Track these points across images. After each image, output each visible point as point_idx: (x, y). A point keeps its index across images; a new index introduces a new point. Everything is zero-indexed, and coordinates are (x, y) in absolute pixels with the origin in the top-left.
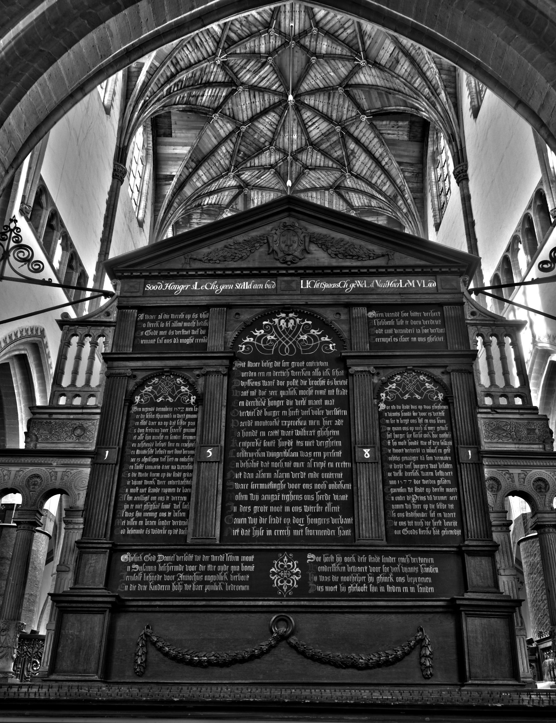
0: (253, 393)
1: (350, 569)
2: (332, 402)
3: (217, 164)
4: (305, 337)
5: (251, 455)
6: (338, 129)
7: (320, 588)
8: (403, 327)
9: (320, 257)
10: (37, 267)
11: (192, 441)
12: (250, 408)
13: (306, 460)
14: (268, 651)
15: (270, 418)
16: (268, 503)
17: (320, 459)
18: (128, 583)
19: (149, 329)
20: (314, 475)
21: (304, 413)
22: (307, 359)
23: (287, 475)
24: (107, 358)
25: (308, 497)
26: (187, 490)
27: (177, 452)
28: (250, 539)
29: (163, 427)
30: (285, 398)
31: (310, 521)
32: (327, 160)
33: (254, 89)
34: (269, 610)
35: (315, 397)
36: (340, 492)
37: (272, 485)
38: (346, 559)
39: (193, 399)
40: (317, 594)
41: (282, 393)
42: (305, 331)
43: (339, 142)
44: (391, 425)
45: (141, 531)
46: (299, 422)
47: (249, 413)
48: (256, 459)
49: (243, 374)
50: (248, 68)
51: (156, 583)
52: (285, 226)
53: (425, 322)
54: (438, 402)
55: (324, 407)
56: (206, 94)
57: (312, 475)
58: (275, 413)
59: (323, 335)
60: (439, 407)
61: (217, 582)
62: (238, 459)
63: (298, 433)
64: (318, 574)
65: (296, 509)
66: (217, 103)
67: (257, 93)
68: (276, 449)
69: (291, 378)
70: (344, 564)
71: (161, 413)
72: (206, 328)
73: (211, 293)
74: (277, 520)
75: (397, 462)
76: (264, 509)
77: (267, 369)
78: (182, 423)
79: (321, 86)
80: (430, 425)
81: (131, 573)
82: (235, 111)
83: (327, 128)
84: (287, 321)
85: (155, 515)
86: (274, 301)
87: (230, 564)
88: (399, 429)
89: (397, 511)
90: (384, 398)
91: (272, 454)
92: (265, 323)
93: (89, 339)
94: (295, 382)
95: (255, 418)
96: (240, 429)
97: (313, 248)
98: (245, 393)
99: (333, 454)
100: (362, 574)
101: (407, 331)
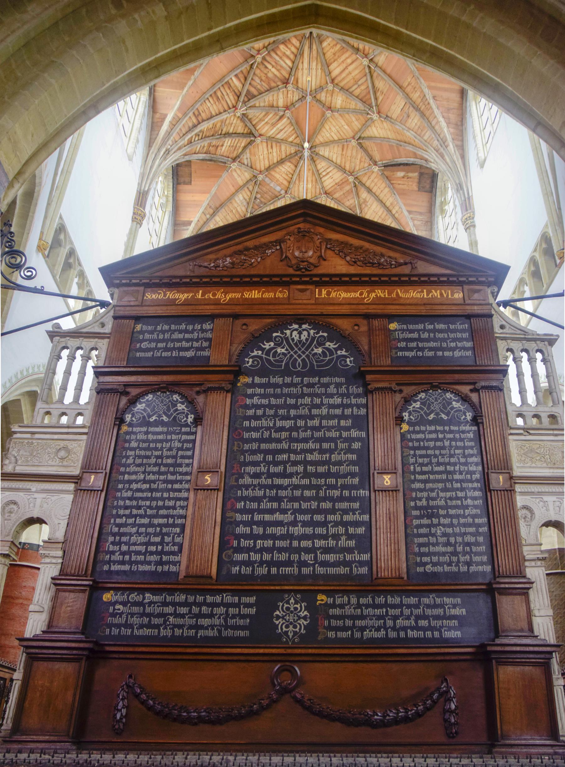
0: (260, 412)
2: (349, 422)
3: (234, 211)
4: (320, 350)
5: (256, 482)
6: (351, 179)
10: (29, 274)
12: (256, 429)
13: (318, 488)
15: (279, 441)
16: (274, 537)
17: (334, 487)
18: (110, 626)
19: (146, 340)
20: (327, 505)
21: (317, 434)
22: (321, 374)
23: (296, 505)
25: (319, 530)
26: (180, 521)
28: (252, 577)
30: (296, 418)
31: (322, 557)
33: (271, 140)
34: (271, 659)
35: (329, 417)
36: (356, 524)
37: (278, 517)
38: (363, 601)
40: (327, 640)
41: (293, 412)
42: (320, 344)
43: (352, 191)
44: (414, 448)
45: (126, 568)
46: (311, 445)
47: (254, 435)
48: (261, 486)
49: (250, 391)
50: (266, 120)
51: (141, 626)
55: (339, 428)
56: (225, 144)
58: (284, 435)
59: (340, 348)
60: (468, 428)
61: (212, 627)
63: (310, 457)
64: (329, 617)
65: (304, 544)
66: (236, 152)
67: (274, 144)
68: (284, 475)
69: (303, 396)
70: (359, 606)
71: (154, 433)
73: (217, 303)
74: (284, 557)
75: (421, 490)
76: (269, 543)
77: (276, 386)
78: (178, 445)
79: (336, 138)
81: (114, 615)
82: (253, 161)
83: (341, 178)
84: (300, 333)
85: (143, 549)
87: (228, 605)
88: (423, 452)
89: (420, 545)
90: (406, 418)
91: (278, 481)
92: (275, 335)
93: (79, 352)
94: (307, 400)
95: (261, 440)
96: (243, 452)
98: (251, 412)
99: (349, 481)
101: (432, 344)
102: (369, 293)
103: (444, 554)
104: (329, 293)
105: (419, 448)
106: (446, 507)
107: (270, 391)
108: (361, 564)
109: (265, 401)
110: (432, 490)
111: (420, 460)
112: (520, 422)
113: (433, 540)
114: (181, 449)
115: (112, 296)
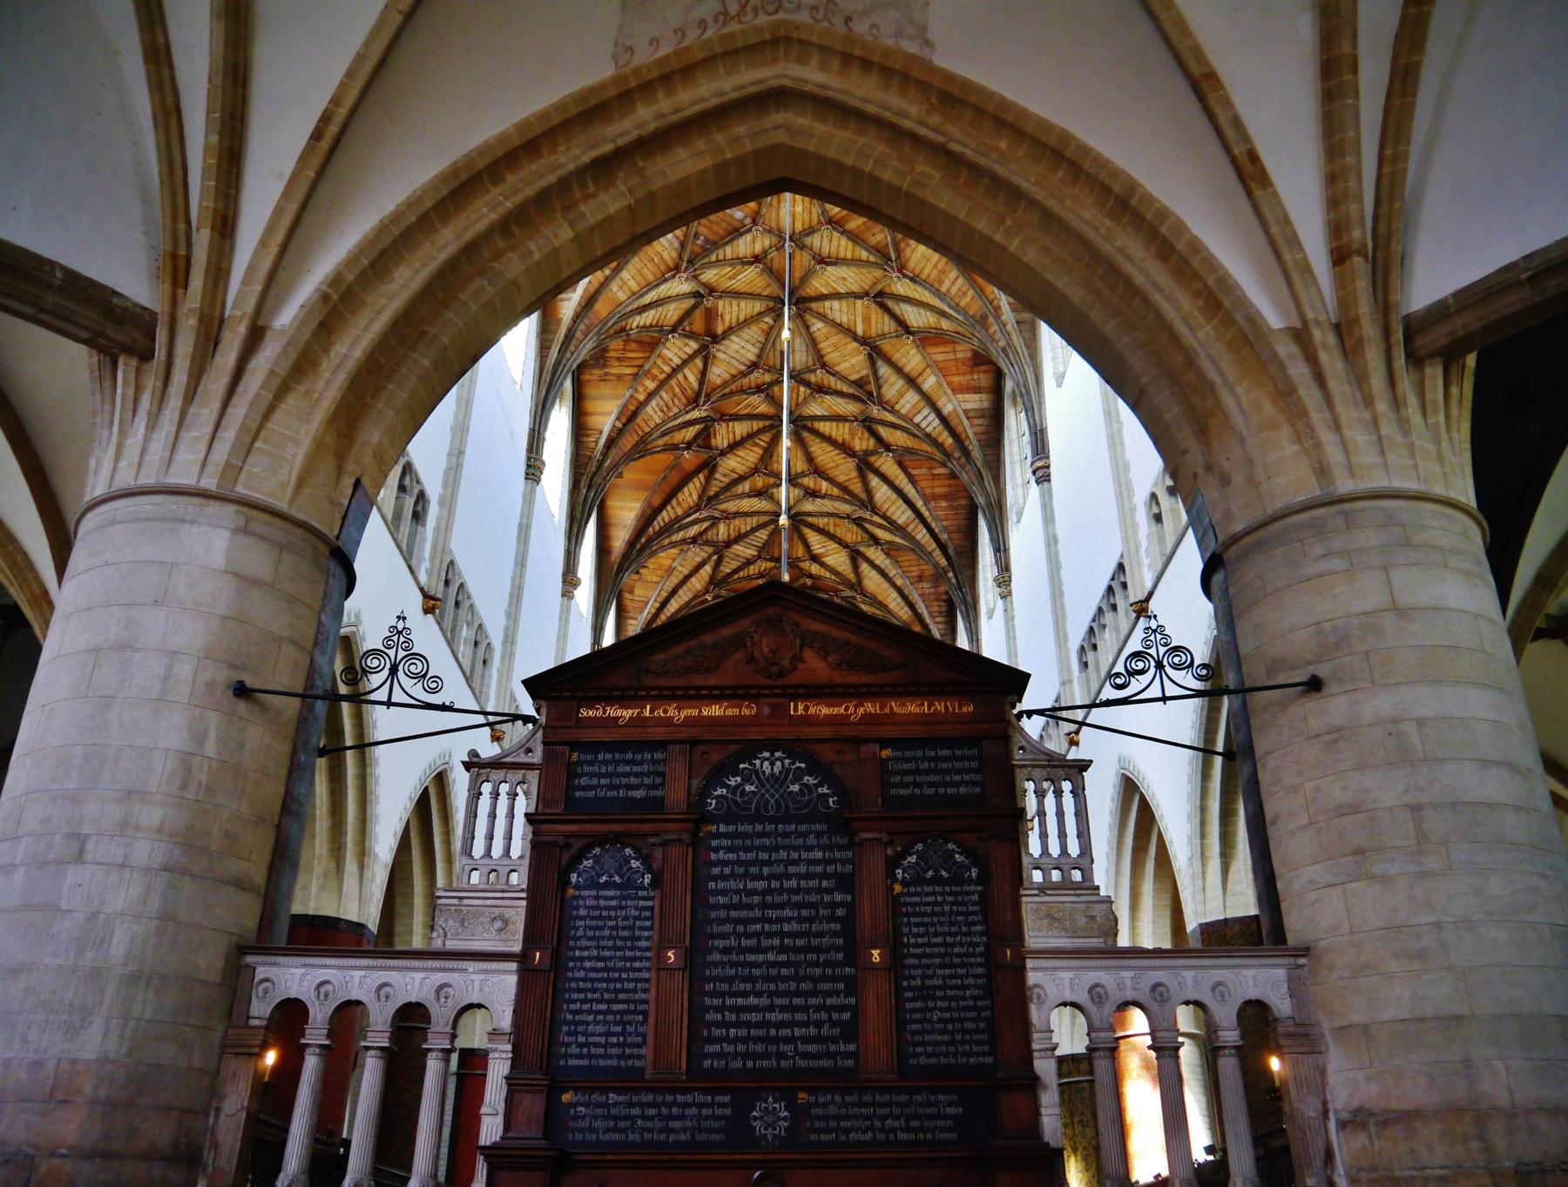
0: (727, 871)
5: (725, 958)
7: (814, 1137)
11: (647, 939)
12: (724, 893)
13: (796, 965)
15: (750, 907)
16: (748, 1025)
17: (815, 964)
18: (574, 1130)
21: (795, 899)
23: (772, 987)
25: (799, 1016)
26: (642, 1007)
27: (628, 954)
29: (609, 918)
30: (769, 877)
32: (857, 249)
35: (809, 876)
36: (841, 1009)
37: (752, 1000)
39: (647, 879)
41: (766, 870)
44: (908, 915)
45: (584, 1062)
46: (787, 912)
47: (721, 900)
48: (733, 964)
49: (714, 843)
51: (607, 1131)
54: (970, 881)
57: (803, 986)
58: (756, 899)
60: (972, 888)
61: (685, 1130)
63: (786, 928)
68: (758, 950)
69: (777, 848)
74: (760, 1048)
75: (915, 967)
76: (743, 1032)
77: (744, 836)
78: (634, 913)
80: (959, 913)
87: (700, 1106)
88: (918, 920)
91: (751, 958)
94: (783, 854)
98: (716, 871)
100: (866, 1118)
105: (915, 915)
106: (944, 988)
107: (738, 842)
108: (848, 1055)
109: (732, 856)
110: (928, 967)
111: (915, 930)
112: (1037, 876)
113: (927, 1026)
114: (637, 918)
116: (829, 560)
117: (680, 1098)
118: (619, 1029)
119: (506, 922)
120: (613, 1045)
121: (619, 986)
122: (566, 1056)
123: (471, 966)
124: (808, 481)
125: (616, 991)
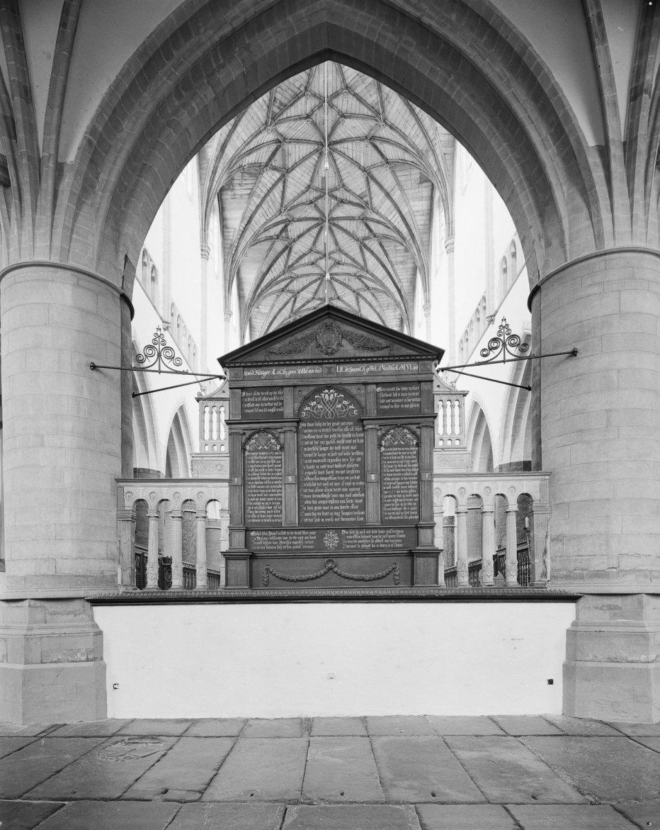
0: (311, 443)
1: (362, 537)
2: (355, 448)
4: (340, 406)
5: (312, 479)
8: (396, 398)
9: (348, 349)
11: (280, 472)
12: (310, 452)
13: (341, 481)
14: (324, 574)
15: (321, 458)
16: (322, 505)
17: (349, 481)
19: (249, 402)
20: (345, 490)
21: (340, 454)
22: (342, 420)
23: (331, 490)
24: (228, 423)
25: (342, 502)
26: (280, 499)
27: (272, 478)
28: (313, 524)
29: (264, 464)
30: (329, 445)
31: (343, 514)
35: (346, 445)
36: (359, 498)
37: (323, 496)
38: (361, 532)
39: (278, 447)
40: (347, 549)
41: (328, 443)
42: (340, 402)
44: (387, 460)
46: (337, 460)
47: (310, 455)
48: (315, 481)
49: (305, 431)
52: (326, 326)
53: (410, 394)
54: (413, 446)
55: (350, 451)
57: (344, 490)
58: (324, 455)
59: (350, 404)
60: (414, 449)
62: (305, 482)
63: (337, 466)
64: (347, 539)
65: (336, 508)
68: (325, 476)
69: (332, 433)
70: (360, 535)
71: (262, 456)
72: (282, 401)
74: (326, 514)
75: (389, 481)
76: (320, 508)
77: (318, 428)
78: (273, 461)
80: (408, 459)
84: (329, 395)
86: (321, 382)
87: (304, 536)
88: (391, 462)
90: (383, 444)
91: (322, 479)
92: (316, 397)
93: (214, 410)
94: (335, 435)
95: (313, 458)
96: (305, 464)
97: (344, 342)
98: (307, 443)
99: (355, 477)
102: (366, 368)
103: (398, 511)
104: (344, 369)
105: (389, 460)
106: (400, 489)
107: (316, 431)
108: (361, 516)
109: (313, 437)
110: (394, 481)
111: (389, 467)
112: (441, 443)
113: (393, 505)
114: (275, 464)
115: (225, 373)
116: (345, 299)
117: (296, 533)
118: (271, 508)
119: (222, 466)
120: (269, 514)
121: (270, 491)
122: (251, 518)
123: (210, 484)
124: (336, 256)
125: (269, 493)
